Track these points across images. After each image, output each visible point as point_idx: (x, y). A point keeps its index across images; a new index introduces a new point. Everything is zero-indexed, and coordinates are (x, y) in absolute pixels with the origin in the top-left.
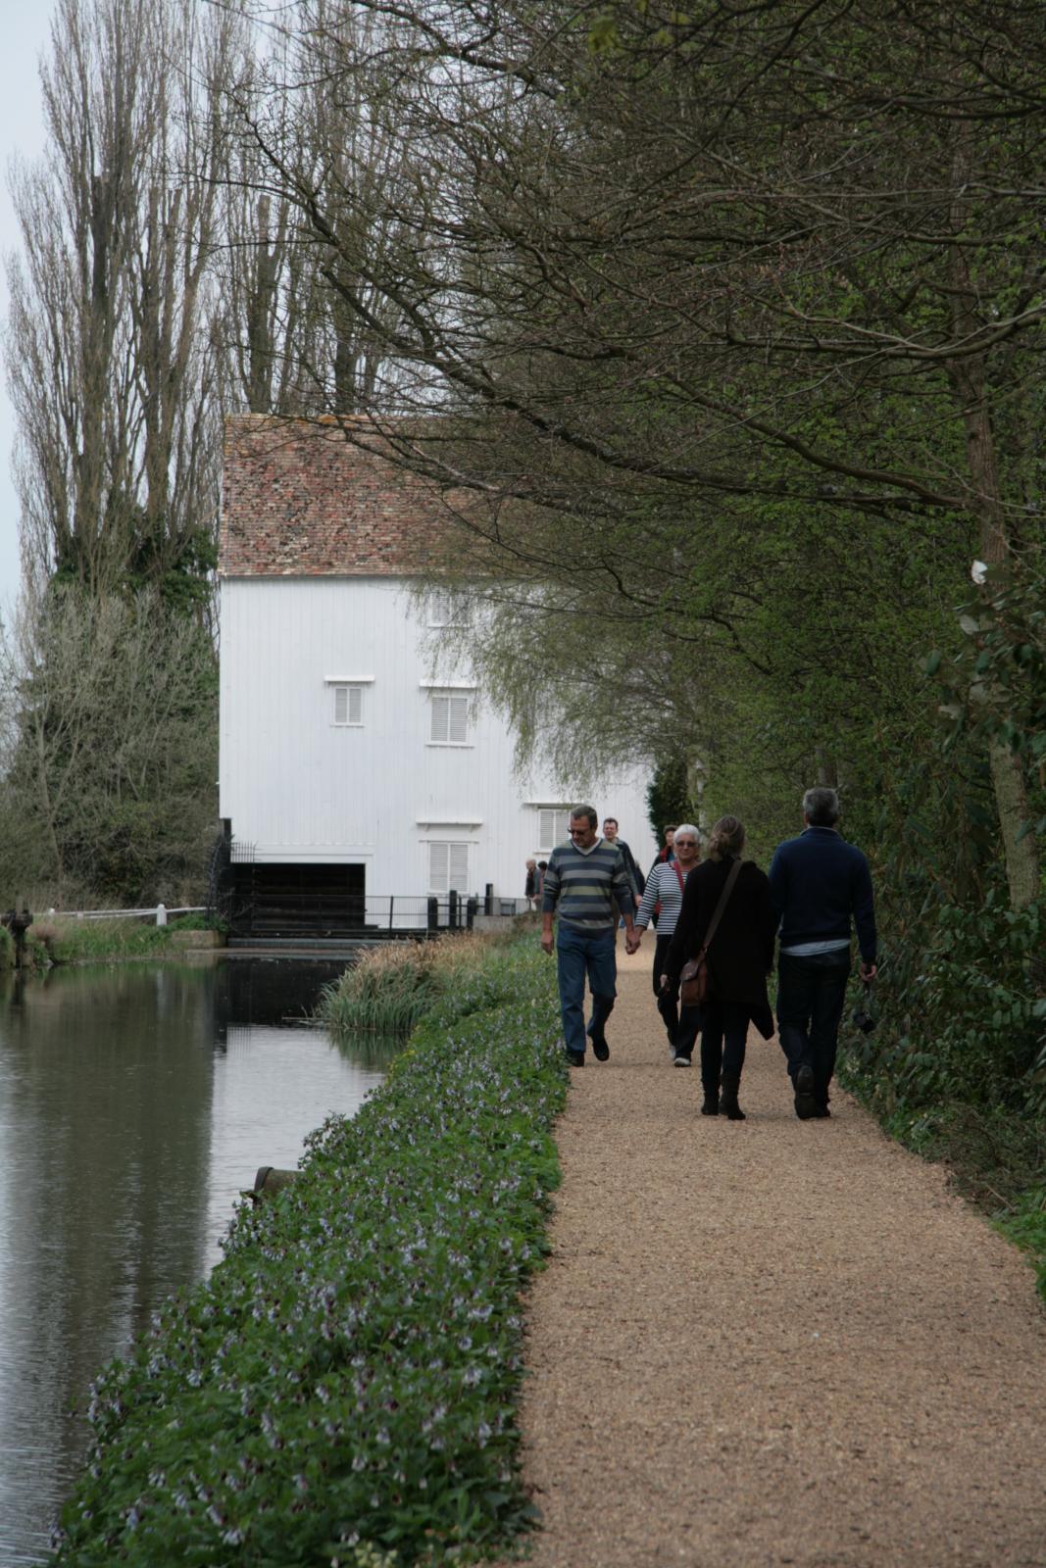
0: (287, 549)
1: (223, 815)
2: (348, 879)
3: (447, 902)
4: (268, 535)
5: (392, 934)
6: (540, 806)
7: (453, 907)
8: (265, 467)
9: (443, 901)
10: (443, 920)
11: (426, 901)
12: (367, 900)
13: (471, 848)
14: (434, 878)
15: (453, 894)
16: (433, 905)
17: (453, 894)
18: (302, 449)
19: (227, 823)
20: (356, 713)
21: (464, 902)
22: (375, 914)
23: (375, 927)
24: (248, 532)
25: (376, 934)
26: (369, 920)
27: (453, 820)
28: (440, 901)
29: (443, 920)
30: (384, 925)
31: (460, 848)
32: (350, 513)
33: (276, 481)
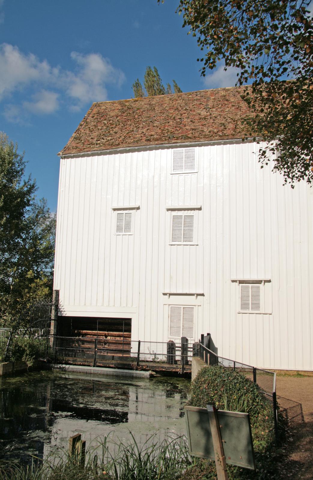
0: (99, 142)
1: (55, 288)
3: (180, 345)
4: (92, 138)
6: (241, 282)
7: (184, 348)
8: (102, 117)
9: (178, 342)
11: (166, 344)
12: (132, 343)
13: (195, 308)
15: (185, 340)
17: (185, 340)
19: (57, 292)
20: (128, 227)
24: (82, 139)
26: (132, 355)
27: (184, 292)
31: (189, 310)
32: (136, 127)
33: (105, 120)
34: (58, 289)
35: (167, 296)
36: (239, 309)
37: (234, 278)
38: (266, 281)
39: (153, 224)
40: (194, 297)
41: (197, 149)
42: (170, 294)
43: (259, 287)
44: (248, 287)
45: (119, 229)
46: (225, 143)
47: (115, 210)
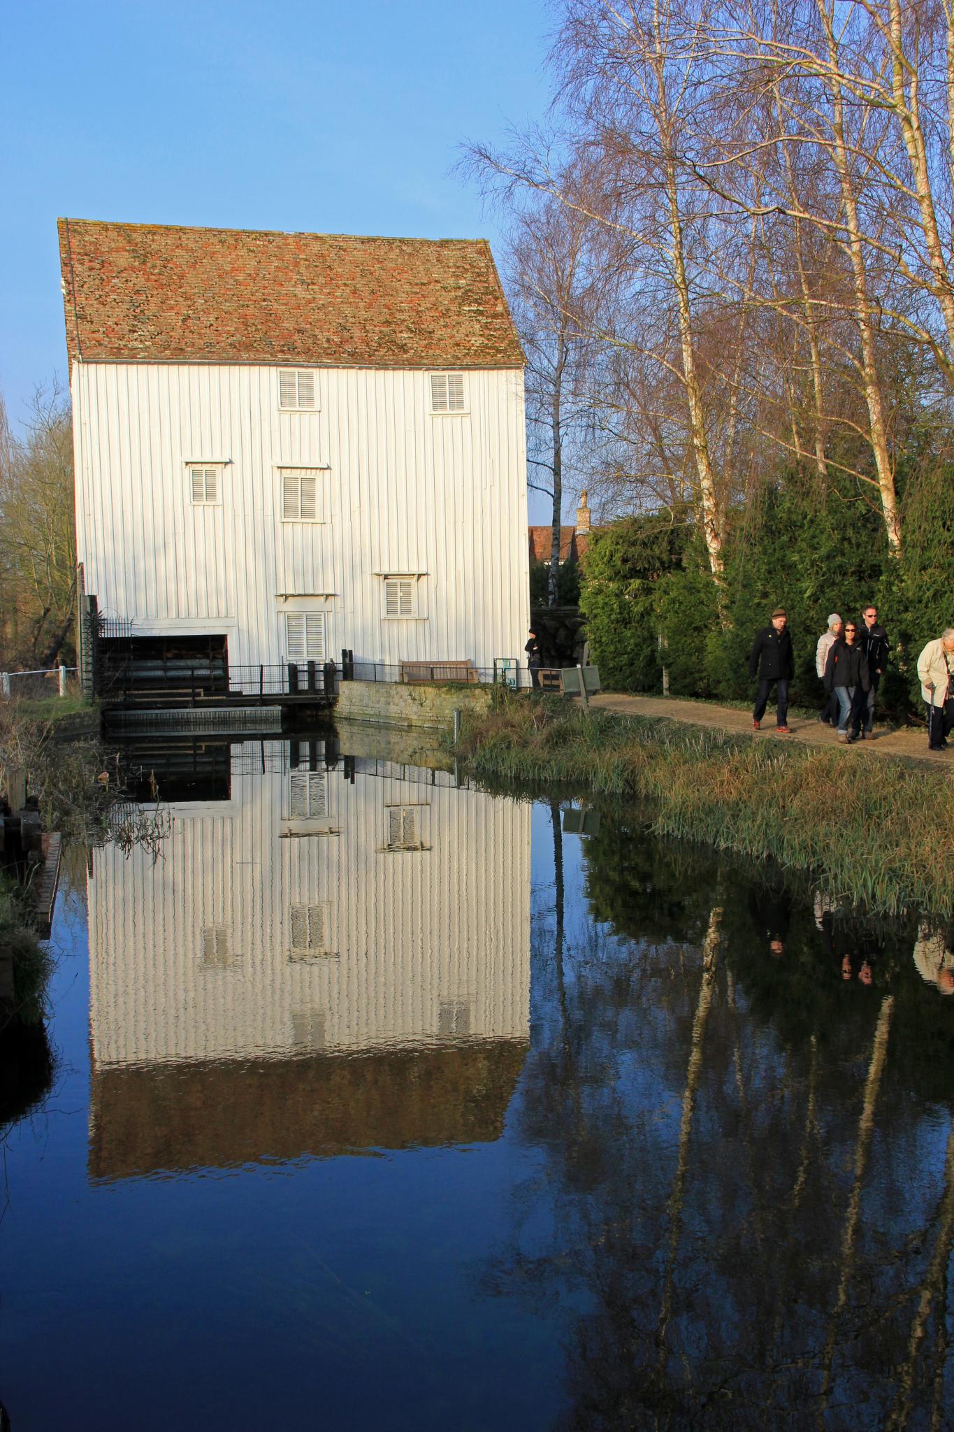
2: (214, 646)
5: (263, 700)
6: (386, 577)
10: (304, 685)
11: (286, 668)
14: (294, 647)
16: (293, 670)
18: (134, 251)
19: (93, 599)
20: (211, 493)
21: (322, 668)
22: (240, 680)
23: (240, 694)
25: (240, 700)
28: (300, 668)
29: (304, 685)
30: (251, 690)
34: (94, 593)
35: (282, 599)
36: (384, 614)
37: (377, 571)
38: (420, 576)
39: (250, 489)
40: (322, 599)
41: (315, 371)
42: (287, 597)
43: (409, 584)
44: (395, 584)
45: (196, 496)
46: (360, 368)
47: (187, 463)
